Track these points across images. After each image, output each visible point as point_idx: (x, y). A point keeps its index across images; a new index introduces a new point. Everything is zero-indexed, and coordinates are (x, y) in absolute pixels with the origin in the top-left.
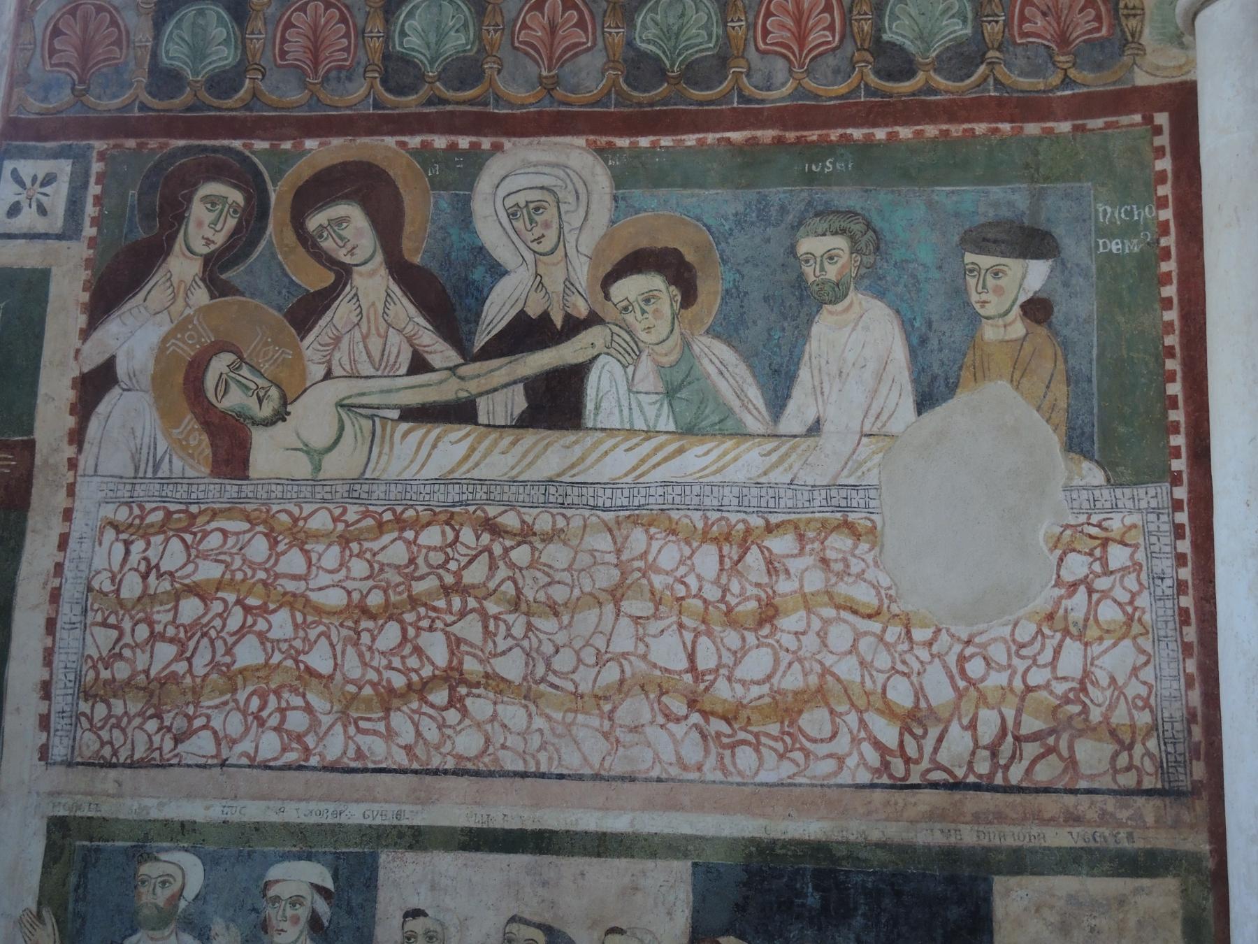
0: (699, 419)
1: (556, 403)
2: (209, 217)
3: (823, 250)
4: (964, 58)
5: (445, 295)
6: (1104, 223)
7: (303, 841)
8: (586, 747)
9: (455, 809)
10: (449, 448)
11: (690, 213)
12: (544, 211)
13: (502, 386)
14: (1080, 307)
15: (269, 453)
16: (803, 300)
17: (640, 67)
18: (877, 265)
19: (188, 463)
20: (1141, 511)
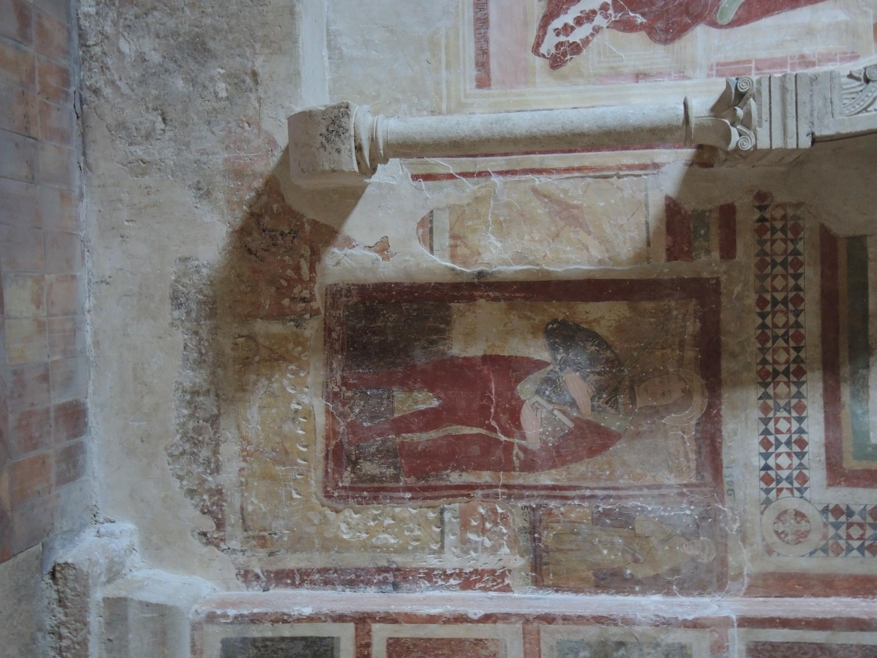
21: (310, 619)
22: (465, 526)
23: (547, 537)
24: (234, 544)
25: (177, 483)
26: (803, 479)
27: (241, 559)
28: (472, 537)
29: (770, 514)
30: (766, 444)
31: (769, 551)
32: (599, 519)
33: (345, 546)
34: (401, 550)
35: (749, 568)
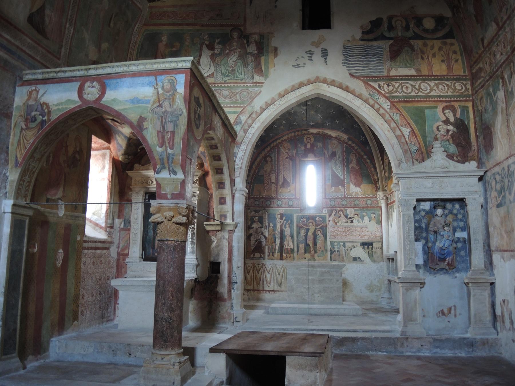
1: (352, 221)
2: (334, 212)
3: (365, 214)
4: (371, 204)
5: (346, 216)
6: (377, 213)
7: (342, 242)
8: (355, 238)
10: (347, 224)
11: (358, 212)
12: (351, 212)
13: (349, 221)
14: (377, 217)
15: (338, 224)
16: (364, 216)
17: (355, 205)
18: (367, 215)
19: (334, 225)
20: (379, 226)
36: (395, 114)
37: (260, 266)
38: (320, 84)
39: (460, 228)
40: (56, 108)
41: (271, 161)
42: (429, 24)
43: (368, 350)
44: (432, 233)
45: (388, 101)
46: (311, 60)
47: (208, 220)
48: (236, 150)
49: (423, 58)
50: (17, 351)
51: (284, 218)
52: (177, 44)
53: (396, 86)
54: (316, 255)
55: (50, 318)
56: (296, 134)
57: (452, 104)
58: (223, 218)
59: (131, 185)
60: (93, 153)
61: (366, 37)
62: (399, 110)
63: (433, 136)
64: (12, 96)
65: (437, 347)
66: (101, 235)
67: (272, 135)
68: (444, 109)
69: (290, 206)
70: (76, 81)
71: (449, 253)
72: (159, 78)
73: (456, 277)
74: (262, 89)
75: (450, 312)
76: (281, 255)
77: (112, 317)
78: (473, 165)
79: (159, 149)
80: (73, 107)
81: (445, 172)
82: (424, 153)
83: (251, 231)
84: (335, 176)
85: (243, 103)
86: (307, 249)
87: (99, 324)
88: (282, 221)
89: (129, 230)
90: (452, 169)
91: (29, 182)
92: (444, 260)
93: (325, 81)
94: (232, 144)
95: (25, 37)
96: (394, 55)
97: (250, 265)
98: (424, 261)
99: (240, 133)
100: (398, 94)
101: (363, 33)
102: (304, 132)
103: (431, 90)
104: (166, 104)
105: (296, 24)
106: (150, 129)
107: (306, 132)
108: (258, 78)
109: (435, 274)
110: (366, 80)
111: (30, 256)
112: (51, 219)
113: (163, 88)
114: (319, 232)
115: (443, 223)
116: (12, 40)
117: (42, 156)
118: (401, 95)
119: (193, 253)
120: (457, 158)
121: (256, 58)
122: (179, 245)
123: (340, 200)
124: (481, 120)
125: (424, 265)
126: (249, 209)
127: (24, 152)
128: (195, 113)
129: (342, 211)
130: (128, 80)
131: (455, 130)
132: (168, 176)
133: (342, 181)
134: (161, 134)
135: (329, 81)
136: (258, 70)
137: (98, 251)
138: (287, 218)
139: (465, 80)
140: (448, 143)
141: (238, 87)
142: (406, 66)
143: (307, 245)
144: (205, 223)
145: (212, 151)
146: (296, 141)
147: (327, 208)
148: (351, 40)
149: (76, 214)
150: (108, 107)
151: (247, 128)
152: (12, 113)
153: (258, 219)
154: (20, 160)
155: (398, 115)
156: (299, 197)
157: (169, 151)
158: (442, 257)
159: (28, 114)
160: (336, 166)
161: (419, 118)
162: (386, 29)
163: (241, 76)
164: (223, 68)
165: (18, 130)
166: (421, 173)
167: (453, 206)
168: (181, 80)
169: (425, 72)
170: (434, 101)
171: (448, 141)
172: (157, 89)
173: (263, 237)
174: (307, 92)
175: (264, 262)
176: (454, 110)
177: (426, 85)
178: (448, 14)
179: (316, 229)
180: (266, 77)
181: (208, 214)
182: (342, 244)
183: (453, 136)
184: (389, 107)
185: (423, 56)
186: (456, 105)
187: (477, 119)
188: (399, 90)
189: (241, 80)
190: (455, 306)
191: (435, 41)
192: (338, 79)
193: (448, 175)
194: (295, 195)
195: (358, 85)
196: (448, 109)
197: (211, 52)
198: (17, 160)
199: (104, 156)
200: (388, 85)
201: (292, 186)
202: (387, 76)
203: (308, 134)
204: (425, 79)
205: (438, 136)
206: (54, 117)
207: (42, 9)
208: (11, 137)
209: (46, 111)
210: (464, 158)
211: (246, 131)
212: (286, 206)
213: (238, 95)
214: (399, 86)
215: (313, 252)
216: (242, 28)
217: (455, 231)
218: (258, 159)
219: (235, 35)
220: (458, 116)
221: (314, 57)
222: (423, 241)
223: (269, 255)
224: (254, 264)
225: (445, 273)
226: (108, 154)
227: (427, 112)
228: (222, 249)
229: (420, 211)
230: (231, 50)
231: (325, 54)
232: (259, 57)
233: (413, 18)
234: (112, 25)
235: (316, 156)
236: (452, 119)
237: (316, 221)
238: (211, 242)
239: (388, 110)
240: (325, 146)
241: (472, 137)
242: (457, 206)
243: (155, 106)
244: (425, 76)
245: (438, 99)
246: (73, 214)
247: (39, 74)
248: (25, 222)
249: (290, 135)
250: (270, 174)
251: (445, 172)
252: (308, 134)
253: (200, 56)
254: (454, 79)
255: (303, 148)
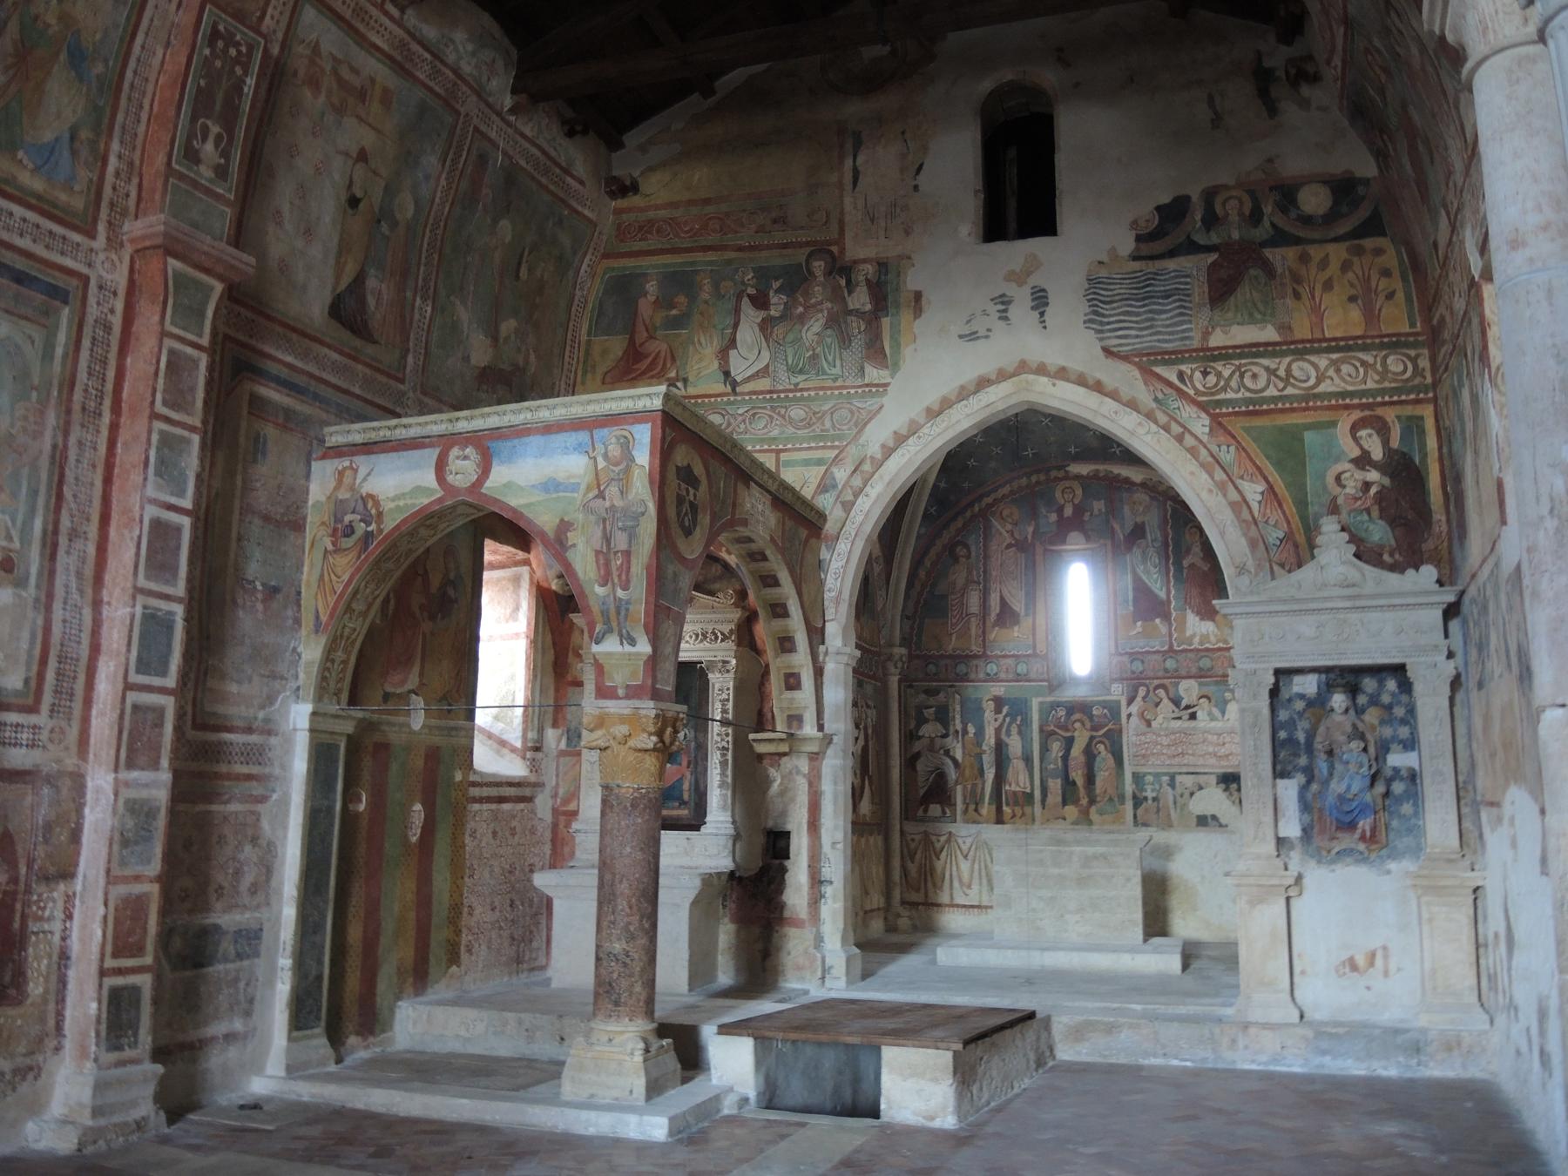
0: (1213, 719)
1: (1193, 717)
2: (1142, 692)
5: (1176, 702)
8: (1201, 762)
9: (1184, 770)
10: (1179, 723)
12: (1189, 690)
15: (1154, 724)
16: (1226, 702)
17: (1201, 669)
19: (1143, 727)
21: (100, 1002)
22: (41, 919)
23: (52, 870)
24: (41, 1059)
25: (9, 1099)
26: (34, 727)
27: (49, 1054)
28: (47, 913)
29: (50, 746)
30: (15, 745)
31: (67, 749)
32: (46, 841)
33: (46, 991)
34: (50, 957)
35: (75, 760)
36: (1224, 448)
37: (943, 839)
38: (1031, 377)
39: (1401, 742)
40: (392, 505)
41: (968, 557)
42: (1314, 201)
43: (1147, 1054)
44: (1323, 756)
45: (1203, 415)
46: (1006, 319)
47: (760, 728)
48: (824, 554)
49: (1297, 296)
50: (323, 1023)
51: (1005, 710)
52: (682, 299)
53: (1226, 373)
54: (1093, 809)
55: (395, 955)
56: (1034, 479)
57: (1379, 411)
58: (795, 723)
59: (581, 648)
60: (486, 575)
61: (1146, 249)
62: (1234, 437)
63: (1326, 499)
64: (303, 482)
65: (1324, 1053)
66: (513, 768)
67: (966, 485)
68: (1354, 429)
69: (1018, 678)
70: (431, 445)
71: (1363, 810)
72: (598, 433)
73: (1389, 872)
74: (885, 400)
75: (1371, 964)
76: (999, 810)
77: (542, 960)
78: (1429, 572)
79: (600, 590)
80: (426, 501)
81: (1349, 598)
82: (1298, 550)
83: (918, 746)
84: (1141, 590)
85: (839, 438)
86: (1069, 794)
87: (510, 974)
88: (1001, 717)
89: (579, 754)
90: (1369, 588)
91: (345, 662)
92: (1351, 826)
93: (1041, 370)
94: (813, 541)
95: (326, 350)
96: (1221, 291)
97: (917, 837)
98: (1304, 830)
99: (834, 514)
100: (1230, 395)
101: (1139, 239)
102: (1054, 474)
103: (1319, 381)
104: (613, 490)
105: (968, 228)
106: (581, 546)
107: (1061, 474)
108: (873, 374)
109: (1333, 862)
110: (1147, 361)
111: (349, 819)
112: (395, 737)
113: (606, 456)
114: (1101, 747)
115: (1349, 729)
116: (299, 364)
117: (370, 606)
118: (1240, 395)
119: (724, 808)
120: (1391, 555)
121: (869, 323)
122: (643, 796)
123: (1158, 657)
124: (1450, 451)
125: (1302, 838)
126: (911, 686)
127: (332, 600)
128: (680, 500)
129: (1162, 686)
130: (535, 441)
131: (1387, 481)
132: (620, 649)
133: (1162, 603)
134: (604, 557)
135: (1052, 369)
136: (876, 352)
137: (506, 807)
138: (1014, 709)
139: (1414, 345)
140: (1366, 517)
141: (826, 398)
142: (1252, 321)
143: (1069, 784)
144: (751, 736)
145: (755, 566)
146: (1032, 500)
147: (1122, 679)
148: (1105, 258)
149: (452, 723)
150: (496, 501)
151: (851, 498)
152: (304, 518)
153: (936, 713)
154: (324, 618)
155: (1232, 449)
156: (1049, 649)
157: (620, 593)
158: (1348, 819)
159: (338, 520)
160: (1144, 561)
161: (1288, 453)
162: (1199, 224)
163: (834, 371)
164: (790, 352)
165: (318, 555)
166: (1285, 601)
167: (1381, 683)
168: (643, 438)
169: (1302, 331)
170: (1330, 408)
171: (1368, 511)
172: (595, 459)
173: (950, 762)
174: (997, 400)
175: (952, 828)
176: (1383, 429)
177: (1306, 365)
178: (1366, 167)
179: (1092, 738)
180: (895, 368)
181: (760, 714)
182: (1165, 779)
183: (1380, 497)
184: (1207, 430)
185: (1300, 290)
186: (1390, 414)
187: (1445, 450)
188: (1233, 384)
189: (835, 380)
190: (1385, 948)
191: (1331, 248)
192: (1075, 365)
193: (1358, 603)
194: (1034, 647)
195: (1125, 377)
196: (1364, 427)
197: (762, 314)
198: (317, 617)
199: (516, 580)
200: (1205, 374)
201: (1026, 623)
202: (1202, 350)
203: (1067, 477)
204: (1302, 349)
205: (1340, 501)
206: (389, 524)
207: (360, 279)
208: (306, 569)
209: (373, 511)
210: (1408, 556)
211: (848, 507)
212: (1011, 676)
213: (828, 417)
214: (1231, 375)
215: (1084, 802)
216: (835, 249)
217: (1384, 748)
218: (933, 552)
219: (819, 266)
220: (1395, 443)
221: (1014, 312)
222: (1300, 779)
223: (965, 811)
224: (925, 832)
225: (1358, 861)
226: (526, 577)
227: (1309, 436)
228: (793, 800)
229: (1290, 700)
230: (806, 308)
231: (1040, 300)
232: (877, 318)
233: (1271, 189)
234: (524, 273)
235: (1088, 538)
236: (1377, 454)
237: (1091, 717)
238: (767, 782)
239: (1205, 439)
240: (1113, 511)
241: (1433, 499)
242: (1391, 685)
243: (591, 495)
244: (1303, 341)
245: (1341, 402)
246: (443, 723)
247: (356, 433)
248: (338, 747)
249: (1015, 484)
250: (964, 590)
251: (1349, 598)
252: (1067, 477)
253: (736, 326)
254: (1382, 346)
255: (1053, 517)
